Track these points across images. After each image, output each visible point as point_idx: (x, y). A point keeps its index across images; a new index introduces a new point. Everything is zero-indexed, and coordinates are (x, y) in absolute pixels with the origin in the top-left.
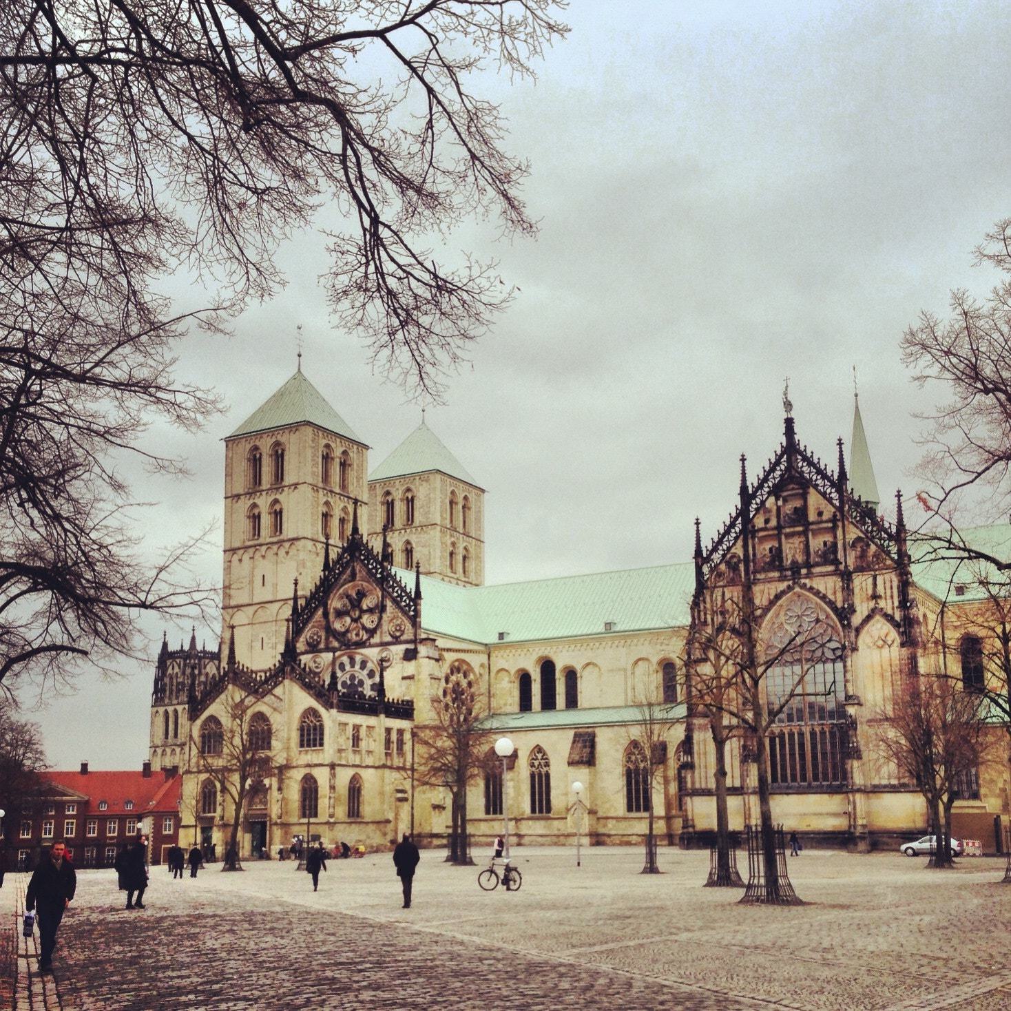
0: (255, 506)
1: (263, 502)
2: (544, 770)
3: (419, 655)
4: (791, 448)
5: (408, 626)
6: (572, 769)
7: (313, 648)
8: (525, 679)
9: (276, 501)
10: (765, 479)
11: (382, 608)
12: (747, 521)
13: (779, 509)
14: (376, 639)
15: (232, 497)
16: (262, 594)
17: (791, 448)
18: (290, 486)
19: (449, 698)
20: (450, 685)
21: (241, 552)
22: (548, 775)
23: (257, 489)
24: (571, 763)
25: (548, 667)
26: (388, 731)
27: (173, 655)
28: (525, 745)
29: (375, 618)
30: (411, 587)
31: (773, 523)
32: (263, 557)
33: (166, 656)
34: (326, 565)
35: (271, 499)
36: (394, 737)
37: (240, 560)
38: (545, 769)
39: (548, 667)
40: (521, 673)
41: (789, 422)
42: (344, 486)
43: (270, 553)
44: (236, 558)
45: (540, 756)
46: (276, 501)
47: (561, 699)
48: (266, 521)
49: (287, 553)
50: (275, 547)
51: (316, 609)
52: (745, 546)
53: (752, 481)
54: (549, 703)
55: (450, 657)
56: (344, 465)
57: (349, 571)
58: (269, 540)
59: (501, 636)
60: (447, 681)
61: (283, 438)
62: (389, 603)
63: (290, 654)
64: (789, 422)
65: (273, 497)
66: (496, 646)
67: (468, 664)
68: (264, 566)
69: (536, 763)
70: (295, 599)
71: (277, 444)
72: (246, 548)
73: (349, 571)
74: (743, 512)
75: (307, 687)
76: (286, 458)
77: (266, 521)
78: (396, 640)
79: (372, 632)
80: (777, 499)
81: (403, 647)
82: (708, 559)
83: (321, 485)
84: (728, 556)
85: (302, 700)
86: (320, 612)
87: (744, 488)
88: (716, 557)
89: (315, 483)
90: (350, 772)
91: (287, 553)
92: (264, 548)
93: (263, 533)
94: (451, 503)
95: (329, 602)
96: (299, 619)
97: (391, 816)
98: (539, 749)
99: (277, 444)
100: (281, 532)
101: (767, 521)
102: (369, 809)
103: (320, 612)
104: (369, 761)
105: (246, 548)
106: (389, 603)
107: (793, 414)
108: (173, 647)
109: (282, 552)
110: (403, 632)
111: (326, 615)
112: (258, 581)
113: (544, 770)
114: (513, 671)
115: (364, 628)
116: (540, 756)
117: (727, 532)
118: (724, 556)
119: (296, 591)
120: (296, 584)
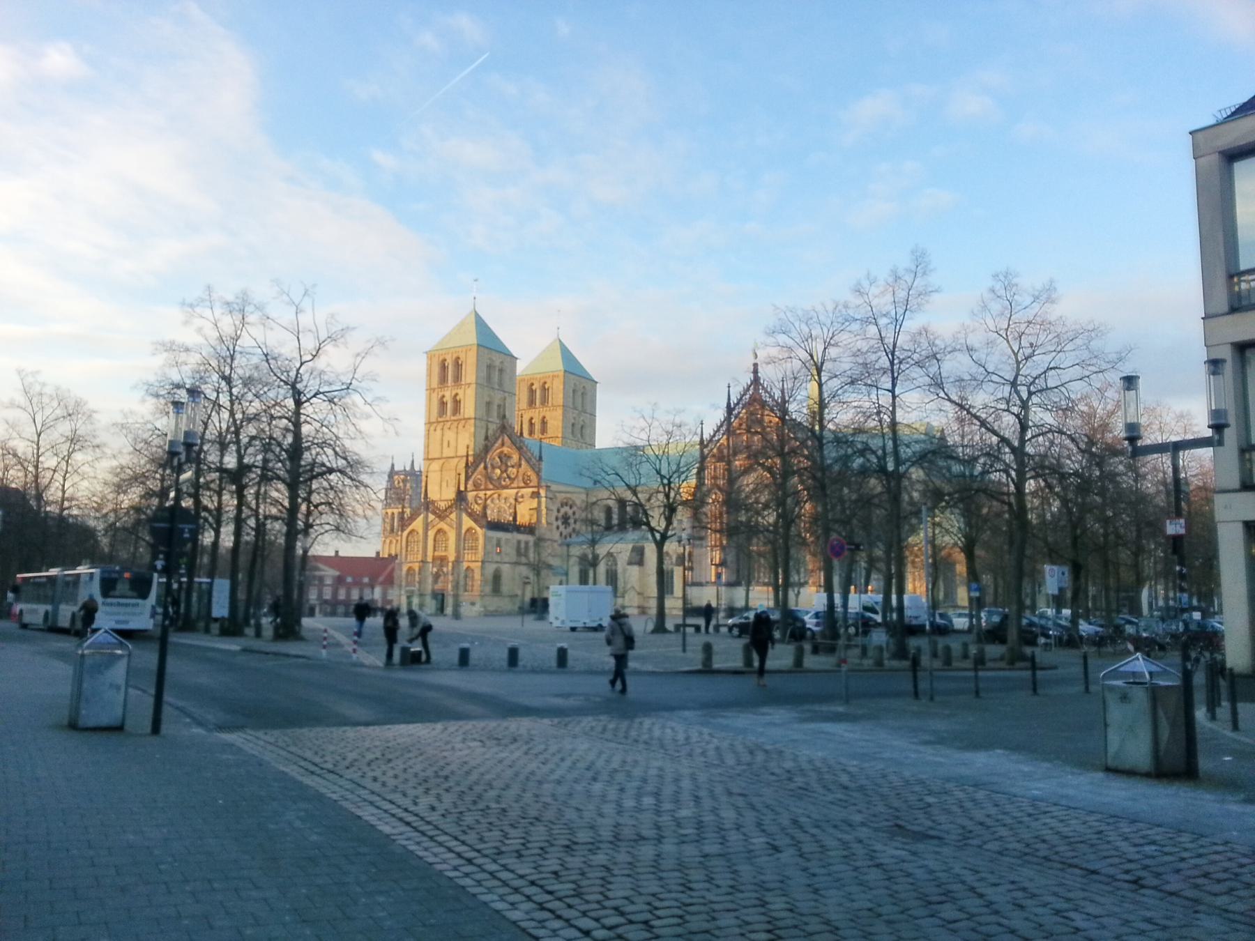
4: (756, 381)
5: (534, 477)
7: (477, 487)
11: (520, 465)
12: (730, 424)
14: (515, 485)
15: (431, 390)
16: (448, 452)
17: (756, 381)
19: (559, 523)
20: (560, 515)
26: (519, 542)
27: (398, 473)
29: (515, 470)
30: (537, 453)
33: (392, 473)
34: (487, 438)
36: (523, 545)
41: (756, 365)
42: (501, 384)
46: (457, 395)
48: (449, 406)
52: (728, 439)
53: (734, 400)
55: (561, 497)
56: (501, 371)
57: (500, 441)
60: (558, 511)
61: (462, 356)
62: (523, 462)
63: (461, 496)
64: (756, 365)
68: (450, 435)
70: (467, 456)
73: (500, 441)
74: (728, 419)
75: (470, 515)
78: (527, 486)
79: (512, 480)
81: (531, 490)
82: (706, 446)
85: (467, 522)
86: (482, 465)
87: (729, 404)
90: (494, 566)
94: (574, 391)
96: (470, 468)
97: (519, 593)
98: (610, 554)
102: (505, 588)
103: (482, 465)
104: (506, 560)
106: (523, 462)
107: (757, 361)
108: (396, 469)
109: (460, 426)
111: (486, 468)
112: (445, 444)
115: (509, 477)
117: (718, 430)
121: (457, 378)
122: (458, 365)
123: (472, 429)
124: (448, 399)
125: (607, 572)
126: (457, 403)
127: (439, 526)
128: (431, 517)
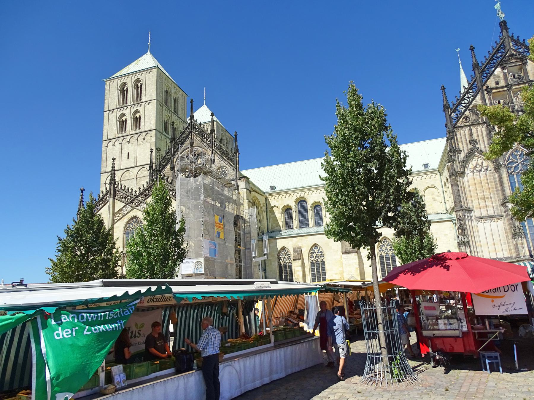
0: (123, 115)
1: (128, 112)
2: (320, 260)
3: (240, 187)
6: (344, 256)
8: (287, 210)
9: (137, 111)
10: (492, 59)
13: (505, 74)
18: (146, 102)
21: (115, 140)
22: (323, 263)
23: (125, 105)
24: (343, 253)
25: (302, 202)
28: (305, 244)
31: (502, 83)
32: (129, 142)
34: (173, 139)
35: (133, 110)
37: (114, 145)
38: (321, 259)
39: (302, 202)
40: (286, 208)
43: (133, 140)
44: (111, 144)
45: (316, 251)
46: (137, 111)
47: (311, 221)
49: (144, 139)
50: (136, 136)
51: (165, 165)
52: (483, 99)
54: (304, 223)
56: (175, 100)
58: (131, 133)
59: (272, 188)
61: (142, 77)
62: (216, 158)
65: (135, 109)
66: (271, 194)
67: (259, 202)
68: (129, 148)
69: (314, 255)
71: (138, 80)
72: (117, 138)
73: (188, 141)
76: (143, 87)
77: (130, 122)
80: (503, 68)
83: (164, 103)
84: (471, 106)
86: (169, 166)
88: (462, 109)
89: (161, 101)
91: (144, 139)
92: (130, 137)
93: (128, 129)
95: (175, 160)
99: (138, 80)
100: (140, 128)
101: (497, 83)
105: (117, 138)
106: (216, 158)
109: (141, 138)
110: (226, 175)
111: (172, 168)
112: (125, 155)
113: (320, 260)
114: (281, 207)
116: (316, 251)
118: (467, 108)
119: (151, 156)
120: (151, 152)
121: (138, 97)
122: (138, 87)
123: (154, 139)
124: (129, 118)
125: (312, 264)
126: (137, 120)
127: (131, 214)
128: (119, 205)
